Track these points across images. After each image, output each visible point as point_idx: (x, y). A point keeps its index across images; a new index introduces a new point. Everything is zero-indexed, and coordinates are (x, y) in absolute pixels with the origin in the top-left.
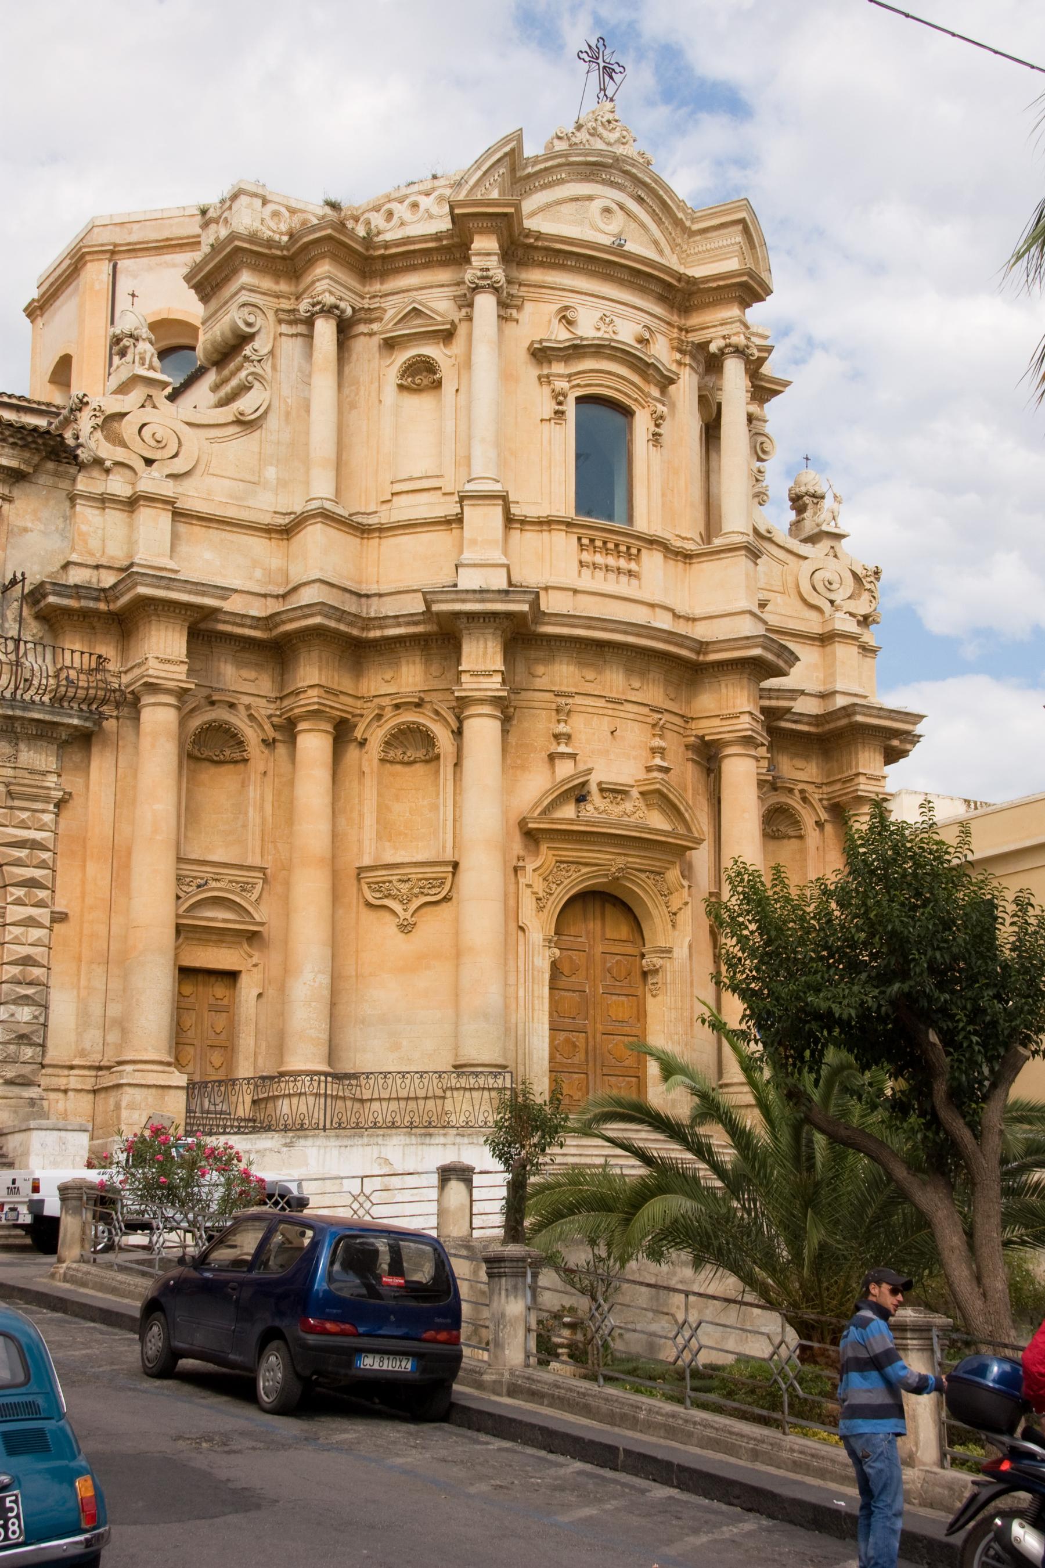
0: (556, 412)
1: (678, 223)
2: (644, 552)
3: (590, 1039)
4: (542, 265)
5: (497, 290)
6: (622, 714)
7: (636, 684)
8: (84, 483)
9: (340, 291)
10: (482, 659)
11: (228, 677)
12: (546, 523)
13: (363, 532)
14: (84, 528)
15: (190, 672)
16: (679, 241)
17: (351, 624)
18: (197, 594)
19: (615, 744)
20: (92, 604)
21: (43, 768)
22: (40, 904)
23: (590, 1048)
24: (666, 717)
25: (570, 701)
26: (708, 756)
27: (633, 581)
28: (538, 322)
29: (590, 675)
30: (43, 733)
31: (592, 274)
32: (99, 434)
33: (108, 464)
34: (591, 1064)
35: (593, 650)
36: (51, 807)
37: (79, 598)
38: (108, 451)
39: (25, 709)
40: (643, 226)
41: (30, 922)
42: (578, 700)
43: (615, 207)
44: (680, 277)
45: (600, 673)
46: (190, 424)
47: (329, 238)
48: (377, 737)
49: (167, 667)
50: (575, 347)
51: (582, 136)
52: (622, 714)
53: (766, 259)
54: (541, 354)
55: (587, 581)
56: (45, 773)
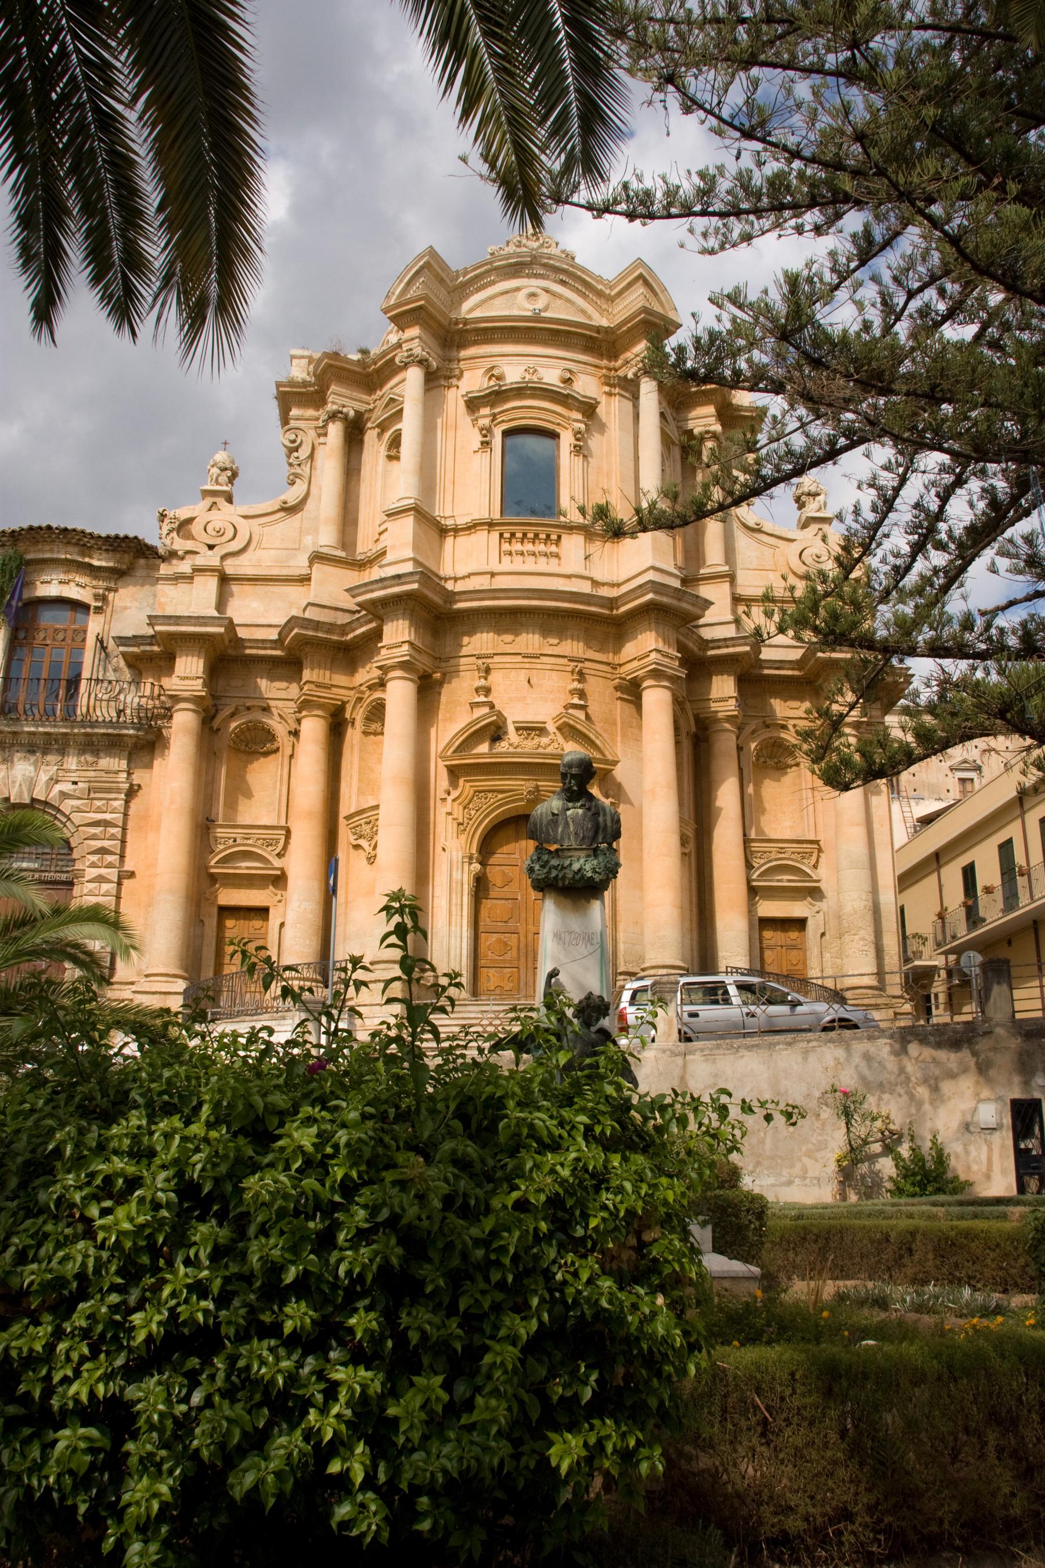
0: (482, 443)
1: (600, 294)
2: (564, 537)
3: (522, 939)
4: (476, 343)
5: (422, 362)
6: (539, 666)
7: (555, 641)
8: (164, 569)
9: (341, 401)
10: (398, 635)
11: (263, 689)
12: (472, 527)
13: (360, 566)
14: (163, 600)
15: (205, 685)
16: (604, 306)
17: (328, 632)
18: (201, 625)
19: (528, 690)
20: (148, 648)
21: (116, 768)
22: (110, 866)
23: (522, 946)
24: (587, 664)
25: (490, 661)
26: (632, 692)
27: (554, 561)
28: (473, 380)
29: (508, 638)
30: (112, 744)
31: (517, 341)
32: (174, 534)
33: (180, 553)
34: (523, 959)
35: (508, 618)
36: (123, 796)
37: (138, 645)
38: (180, 545)
39: (92, 727)
40: (568, 301)
41: (100, 879)
42: (497, 659)
43: (539, 291)
44: (598, 329)
45: (517, 635)
46: (245, 517)
47: (329, 366)
48: (359, 715)
49: (187, 682)
50: (497, 393)
51: (512, 249)
52: (539, 666)
53: (670, 300)
54: (473, 404)
55: (507, 565)
56: (117, 772)
